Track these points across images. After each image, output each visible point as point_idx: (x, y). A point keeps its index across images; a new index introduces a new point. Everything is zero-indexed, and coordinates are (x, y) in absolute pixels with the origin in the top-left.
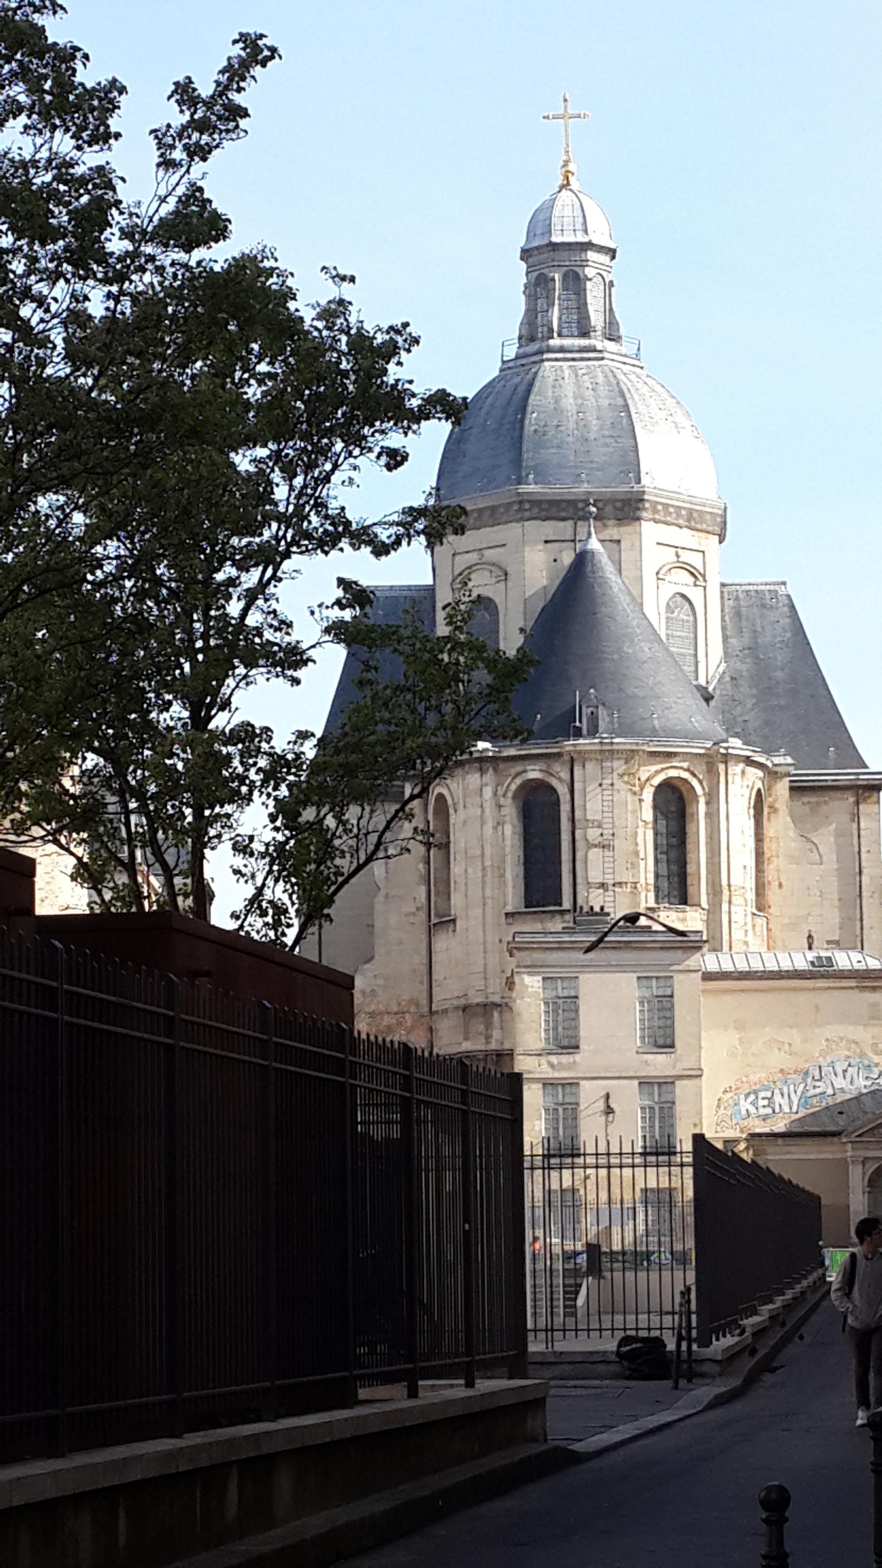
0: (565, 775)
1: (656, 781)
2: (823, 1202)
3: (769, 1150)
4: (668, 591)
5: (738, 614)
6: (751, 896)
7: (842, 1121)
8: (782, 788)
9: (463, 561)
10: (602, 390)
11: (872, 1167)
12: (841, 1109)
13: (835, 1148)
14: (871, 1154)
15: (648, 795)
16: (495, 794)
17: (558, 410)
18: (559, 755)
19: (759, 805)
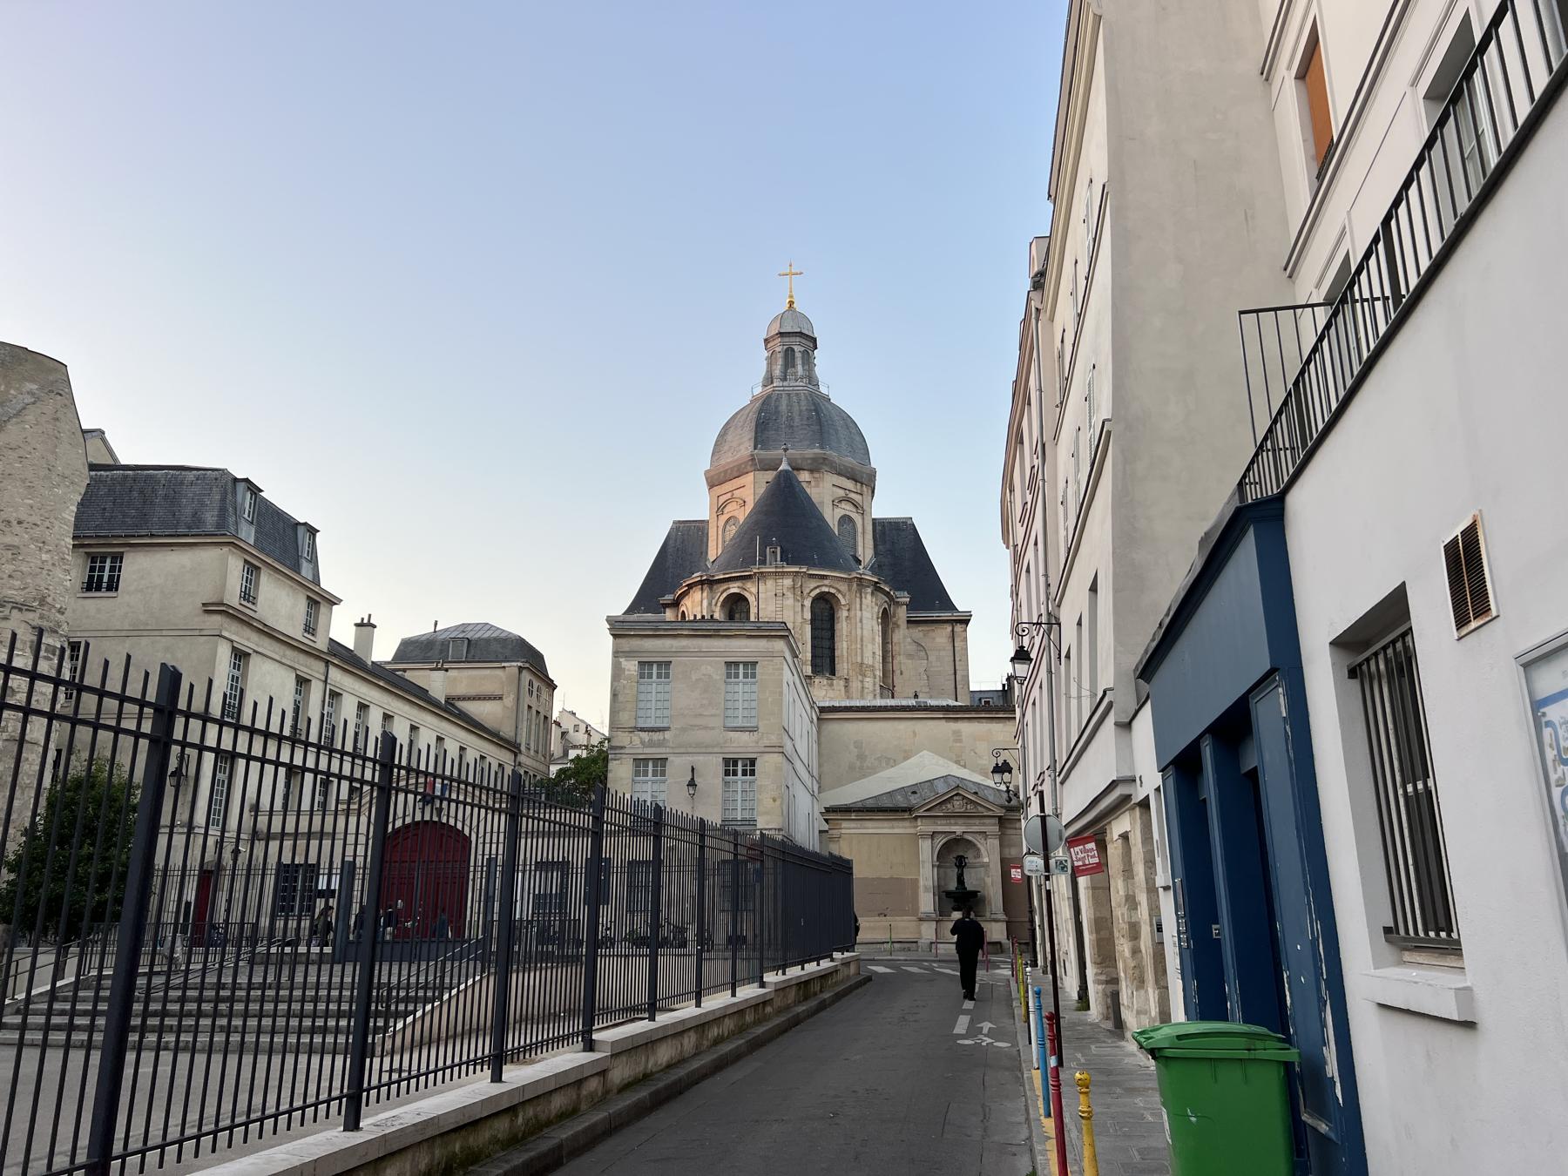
0: (754, 590)
1: (813, 594)
2: (858, 872)
3: (845, 824)
4: (839, 513)
5: (883, 533)
6: (879, 673)
7: (914, 800)
8: (902, 614)
9: (722, 499)
10: (803, 403)
11: (940, 841)
12: (914, 790)
13: (907, 824)
14: (940, 829)
15: (808, 603)
16: (710, 604)
17: (777, 412)
18: (749, 577)
19: (886, 618)
